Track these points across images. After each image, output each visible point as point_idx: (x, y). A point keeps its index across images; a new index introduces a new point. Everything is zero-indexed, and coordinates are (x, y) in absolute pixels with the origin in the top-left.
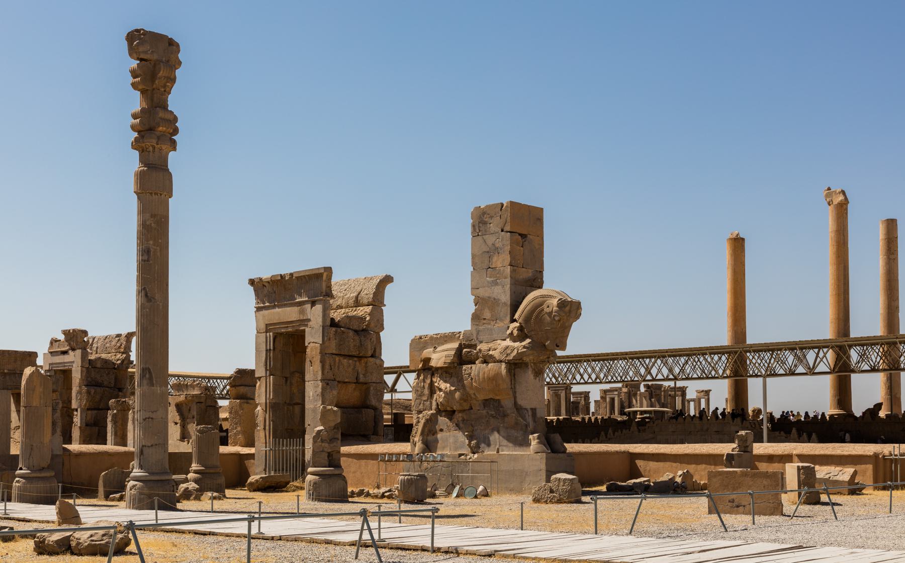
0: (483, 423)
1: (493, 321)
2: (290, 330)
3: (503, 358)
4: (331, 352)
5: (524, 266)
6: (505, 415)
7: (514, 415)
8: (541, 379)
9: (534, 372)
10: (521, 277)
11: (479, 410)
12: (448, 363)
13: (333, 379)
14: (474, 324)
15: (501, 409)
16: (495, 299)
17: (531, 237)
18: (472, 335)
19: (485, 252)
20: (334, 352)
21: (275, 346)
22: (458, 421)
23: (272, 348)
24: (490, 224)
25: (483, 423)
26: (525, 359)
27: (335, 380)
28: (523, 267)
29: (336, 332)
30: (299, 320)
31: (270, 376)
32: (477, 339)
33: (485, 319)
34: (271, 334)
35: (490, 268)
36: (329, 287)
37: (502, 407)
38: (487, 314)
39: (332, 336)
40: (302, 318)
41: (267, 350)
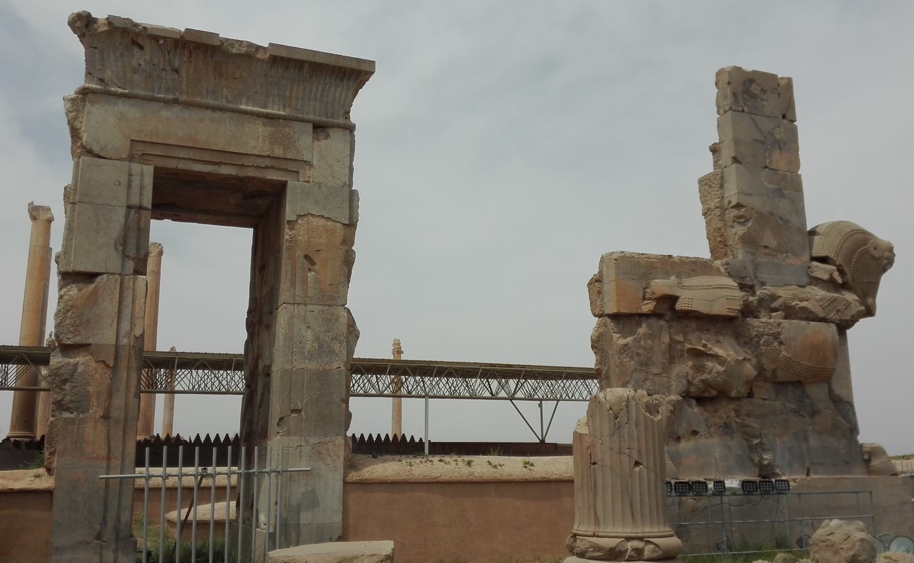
0: (778, 423)
1: (782, 253)
2: (225, 170)
3: (832, 315)
6: (814, 413)
7: (830, 411)
11: (765, 399)
12: (736, 310)
14: (747, 252)
15: (807, 400)
16: (781, 218)
18: (745, 268)
19: (757, 140)
22: (727, 418)
24: (762, 100)
25: (778, 423)
30: (268, 156)
32: (756, 277)
33: (766, 247)
34: (149, 170)
35: (766, 167)
37: (808, 397)
38: (769, 239)
40: (278, 152)
41: (129, 207)
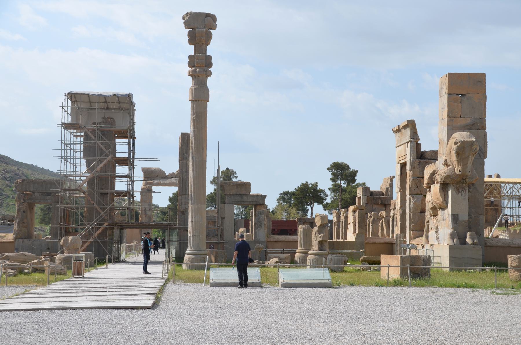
4: (416, 176)
5: (462, 116)
8: (464, 194)
9: (456, 189)
10: (459, 124)
13: (420, 194)
17: (470, 95)
20: (418, 176)
21: (402, 173)
23: (400, 174)
26: (446, 181)
27: (421, 194)
28: (461, 117)
29: (420, 162)
31: (399, 192)
36: (415, 133)
39: (416, 166)
